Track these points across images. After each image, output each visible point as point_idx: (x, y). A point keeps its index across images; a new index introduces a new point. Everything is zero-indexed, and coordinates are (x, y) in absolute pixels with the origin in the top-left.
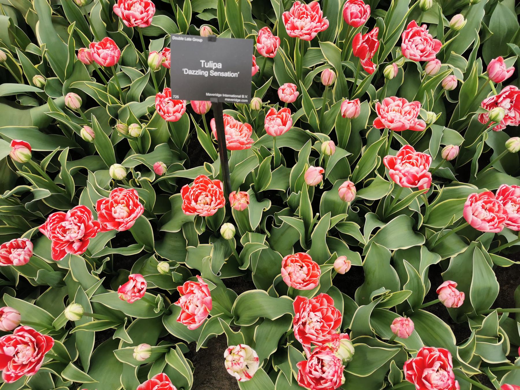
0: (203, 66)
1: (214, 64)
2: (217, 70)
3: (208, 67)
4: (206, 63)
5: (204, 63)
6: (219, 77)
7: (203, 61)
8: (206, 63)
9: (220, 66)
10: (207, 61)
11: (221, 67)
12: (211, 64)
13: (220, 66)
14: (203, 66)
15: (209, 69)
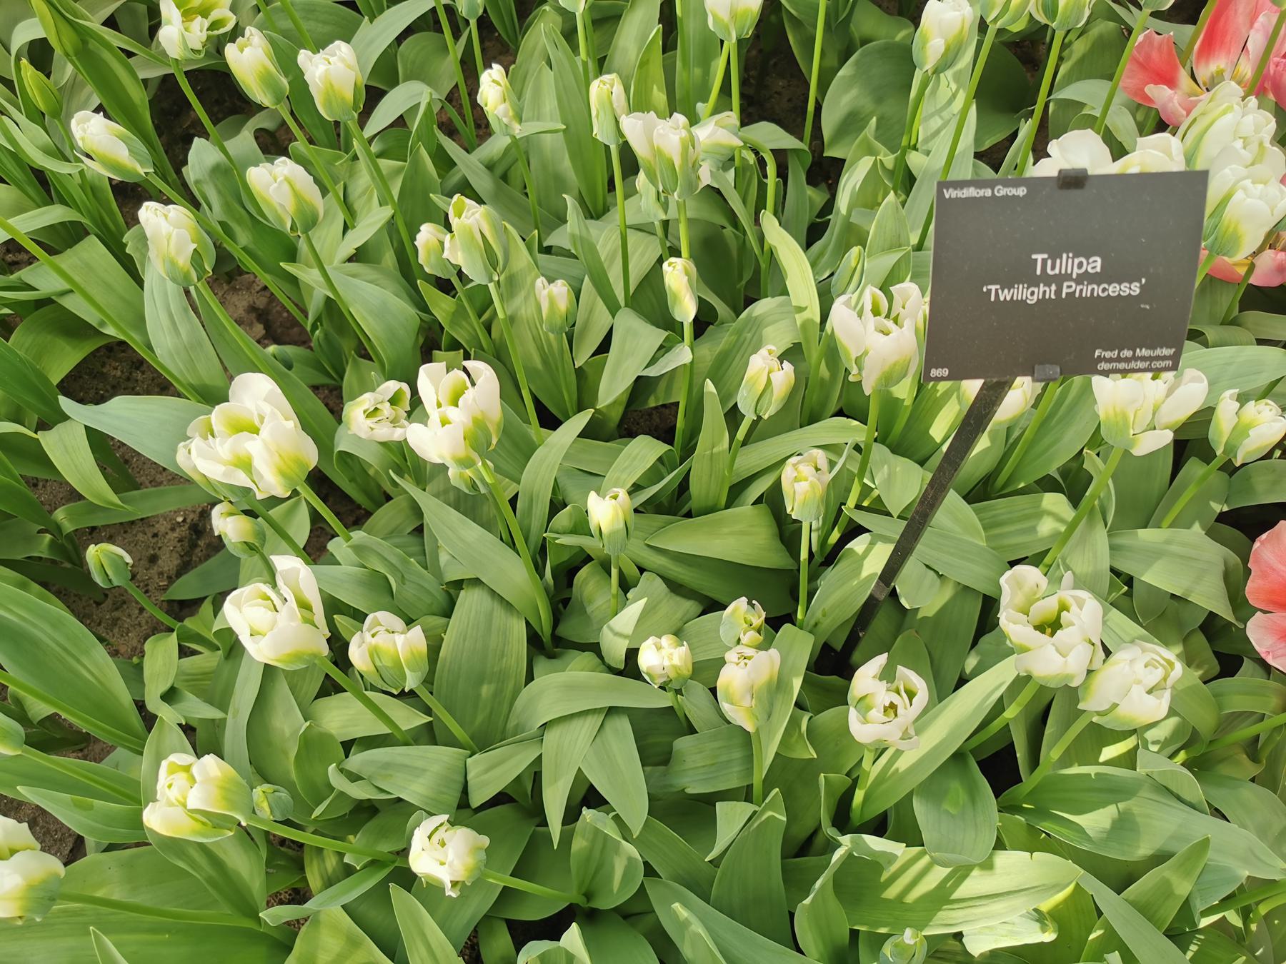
0: (1038, 272)
1: (1076, 261)
2: (1085, 278)
3: (1057, 271)
4: (1049, 262)
5: (1044, 261)
6: (1093, 299)
7: (1039, 257)
8: (1049, 262)
9: (1096, 264)
10: (1055, 256)
11: (1098, 269)
12: (1069, 264)
13: (1095, 264)
14: (1038, 272)
15: (1060, 279)
